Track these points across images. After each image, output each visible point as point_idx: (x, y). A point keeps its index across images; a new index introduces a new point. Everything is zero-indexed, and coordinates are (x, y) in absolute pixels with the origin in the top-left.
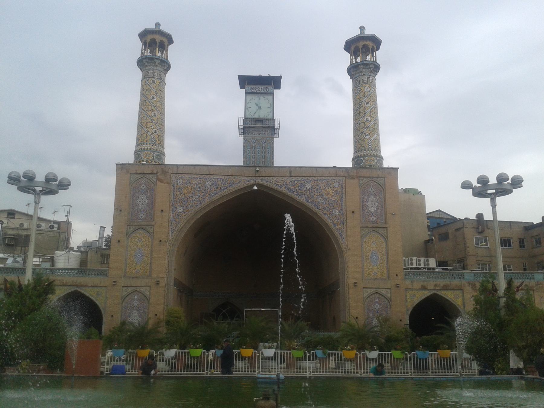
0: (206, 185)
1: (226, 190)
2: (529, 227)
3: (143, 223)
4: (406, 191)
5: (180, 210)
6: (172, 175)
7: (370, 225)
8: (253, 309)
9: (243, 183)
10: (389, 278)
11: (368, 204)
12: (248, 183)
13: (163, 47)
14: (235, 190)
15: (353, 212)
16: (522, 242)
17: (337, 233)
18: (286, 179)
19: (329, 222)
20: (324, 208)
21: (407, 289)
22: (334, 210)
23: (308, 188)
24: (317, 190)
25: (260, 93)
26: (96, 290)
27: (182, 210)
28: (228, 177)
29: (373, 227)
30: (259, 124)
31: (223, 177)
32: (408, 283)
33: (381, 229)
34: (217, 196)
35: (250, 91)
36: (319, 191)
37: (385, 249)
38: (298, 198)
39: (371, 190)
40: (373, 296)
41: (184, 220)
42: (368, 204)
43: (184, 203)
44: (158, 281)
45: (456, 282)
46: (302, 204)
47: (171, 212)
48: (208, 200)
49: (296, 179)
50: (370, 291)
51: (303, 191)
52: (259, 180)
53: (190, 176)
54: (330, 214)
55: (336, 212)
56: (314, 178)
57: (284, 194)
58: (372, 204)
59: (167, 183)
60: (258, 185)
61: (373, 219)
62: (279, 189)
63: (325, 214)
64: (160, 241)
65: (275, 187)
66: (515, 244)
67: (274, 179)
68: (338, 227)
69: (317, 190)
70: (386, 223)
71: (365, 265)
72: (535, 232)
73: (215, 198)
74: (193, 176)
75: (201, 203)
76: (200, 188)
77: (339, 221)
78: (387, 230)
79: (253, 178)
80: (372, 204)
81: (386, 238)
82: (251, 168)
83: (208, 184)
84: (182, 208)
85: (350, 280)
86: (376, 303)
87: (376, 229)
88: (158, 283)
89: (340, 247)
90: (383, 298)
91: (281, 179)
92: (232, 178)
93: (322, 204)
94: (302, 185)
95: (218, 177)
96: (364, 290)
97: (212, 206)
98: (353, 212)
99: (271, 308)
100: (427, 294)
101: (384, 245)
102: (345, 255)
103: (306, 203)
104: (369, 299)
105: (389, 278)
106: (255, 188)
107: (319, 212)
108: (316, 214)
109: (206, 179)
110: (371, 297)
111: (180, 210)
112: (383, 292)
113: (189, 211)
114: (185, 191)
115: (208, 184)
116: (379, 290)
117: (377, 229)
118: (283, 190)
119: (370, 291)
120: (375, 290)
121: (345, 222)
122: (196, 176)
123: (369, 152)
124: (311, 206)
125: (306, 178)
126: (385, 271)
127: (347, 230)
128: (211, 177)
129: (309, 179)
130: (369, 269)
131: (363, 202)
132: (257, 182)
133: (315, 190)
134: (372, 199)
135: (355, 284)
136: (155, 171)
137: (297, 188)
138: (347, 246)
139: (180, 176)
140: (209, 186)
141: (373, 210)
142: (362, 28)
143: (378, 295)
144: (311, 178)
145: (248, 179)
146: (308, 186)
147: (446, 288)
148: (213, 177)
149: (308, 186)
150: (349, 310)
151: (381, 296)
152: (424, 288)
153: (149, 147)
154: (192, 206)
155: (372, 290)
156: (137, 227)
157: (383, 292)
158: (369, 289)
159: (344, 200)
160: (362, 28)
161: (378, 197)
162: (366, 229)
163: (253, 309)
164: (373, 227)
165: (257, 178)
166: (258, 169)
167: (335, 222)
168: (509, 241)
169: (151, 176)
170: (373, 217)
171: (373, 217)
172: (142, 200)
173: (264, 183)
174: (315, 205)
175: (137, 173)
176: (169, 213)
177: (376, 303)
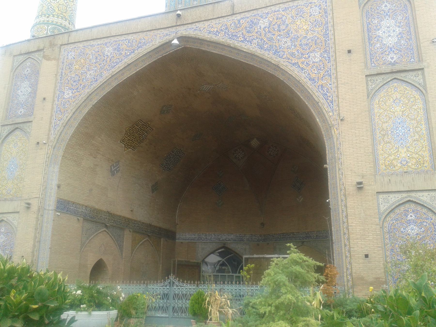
0: (106, 53)
1: (133, 55)
3: (20, 120)
6: (62, 47)
7: (384, 69)
8: (255, 256)
9: (157, 40)
11: (380, 33)
12: (165, 40)
14: (145, 52)
15: (349, 52)
17: (317, 95)
18: (225, 20)
20: (293, 54)
22: (312, 55)
23: (263, 27)
24: (279, 26)
27: (71, 95)
28: (135, 36)
29: (392, 72)
31: (130, 37)
33: (411, 73)
34: (121, 66)
36: (283, 27)
37: (422, 112)
38: (246, 47)
40: (402, 208)
41: (71, 108)
42: (380, 33)
43: (75, 84)
44: (29, 204)
47: (56, 99)
48: (106, 75)
49: (242, 15)
51: (254, 34)
52: (184, 31)
53: (86, 44)
54: (303, 63)
55: (316, 57)
56: (273, 8)
58: (389, 32)
59: (54, 59)
60: (178, 39)
61: (392, 57)
63: (294, 64)
64: (38, 143)
67: (207, 23)
68: (320, 82)
69: (279, 26)
70: (420, 60)
71: (380, 147)
73: (116, 69)
74: (88, 43)
75: (96, 81)
76: (97, 58)
77: (322, 73)
78: (423, 74)
79: (173, 29)
80: (389, 32)
81: (422, 89)
82: (171, 15)
83: (109, 50)
84: (70, 92)
86: (409, 222)
87: (398, 76)
88: (28, 206)
89: (325, 120)
90: (425, 210)
91: (217, 21)
92: (141, 35)
93: (289, 48)
94: (253, 24)
95: (122, 38)
96: (381, 196)
97: (114, 84)
98: (349, 52)
101: (420, 104)
102: (335, 132)
104: (392, 215)
106: (175, 42)
107: (283, 63)
108: (278, 66)
109: (106, 44)
110: (397, 211)
111: (68, 94)
112: (424, 199)
113: (80, 95)
114: (77, 67)
115: (109, 50)
116: (413, 194)
117: (403, 75)
118: (221, 38)
119: (394, 199)
120: (404, 195)
121: (333, 71)
122: (92, 43)
124: (268, 55)
125: (259, 12)
127: (337, 87)
128: (113, 39)
129: (265, 11)
130: (390, 155)
131: (369, 30)
132: (179, 35)
133: (276, 27)
134: (387, 22)
135: (360, 186)
136: (41, 47)
137: (244, 32)
138: (339, 114)
139: (73, 46)
140: (109, 54)
141: (391, 41)
143: (413, 206)
144: (268, 10)
145: (165, 32)
146: (263, 23)
148: (115, 39)
150: (348, 239)
151: (419, 208)
154: (84, 87)
155: (400, 196)
156: (12, 127)
158: (392, 196)
159: (331, 33)
161: (400, 18)
162: (379, 79)
163: (255, 256)
164: (392, 72)
165: (179, 28)
166: (179, 12)
167: (313, 76)
169: (36, 55)
170: (392, 55)
171: (392, 55)
172: (24, 89)
174: (276, 52)
175: (21, 54)
176: (54, 101)
177: (409, 222)
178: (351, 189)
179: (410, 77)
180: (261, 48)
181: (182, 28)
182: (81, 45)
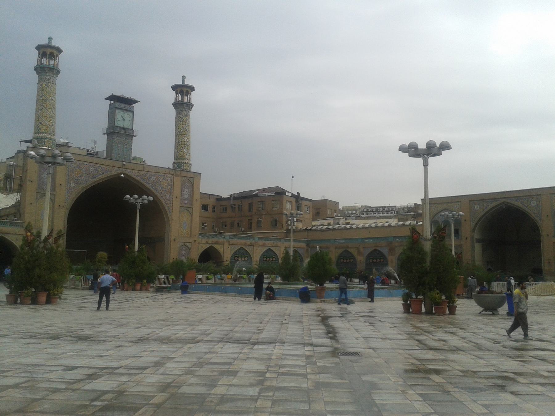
2: (219, 199)
4: (134, 158)
5: (73, 185)
10: (191, 236)
13: (52, 56)
16: (214, 207)
17: (167, 209)
19: (164, 203)
21: (199, 243)
25: (126, 110)
26: (16, 236)
30: (123, 132)
32: (200, 239)
34: (98, 178)
35: (118, 107)
39: (186, 184)
45: (222, 240)
46: (149, 189)
50: (181, 244)
52: (125, 171)
55: (168, 196)
57: (138, 182)
61: (186, 202)
62: (136, 178)
65: (134, 177)
66: (210, 209)
70: (192, 205)
72: (224, 203)
73: (95, 180)
80: (186, 192)
81: (191, 214)
83: (92, 169)
85: (173, 238)
92: (107, 167)
94: (150, 177)
99: (80, 249)
100: (208, 246)
103: (152, 189)
105: (191, 236)
106: (122, 176)
111: (73, 185)
115: (92, 169)
118: (138, 179)
119: (181, 244)
122: (83, 163)
123: (184, 161)
126: (189, 232)
128: (94, 164)
134: (186, 190)
142: (184, 77)
146: (153, 178)
147: (217, 243)
149: (153, 178)
152: (207, 243)
153: (48, 136)
154: (81, 183)
157: (188, 244)
160: (184, 77)
166: (125, 163)
168: (207, 206)
173: (128, 173)
178: (172, 240)
179: (189, 209)
180: (152, 187)
181: (124, 170)
182: (78, 162)
